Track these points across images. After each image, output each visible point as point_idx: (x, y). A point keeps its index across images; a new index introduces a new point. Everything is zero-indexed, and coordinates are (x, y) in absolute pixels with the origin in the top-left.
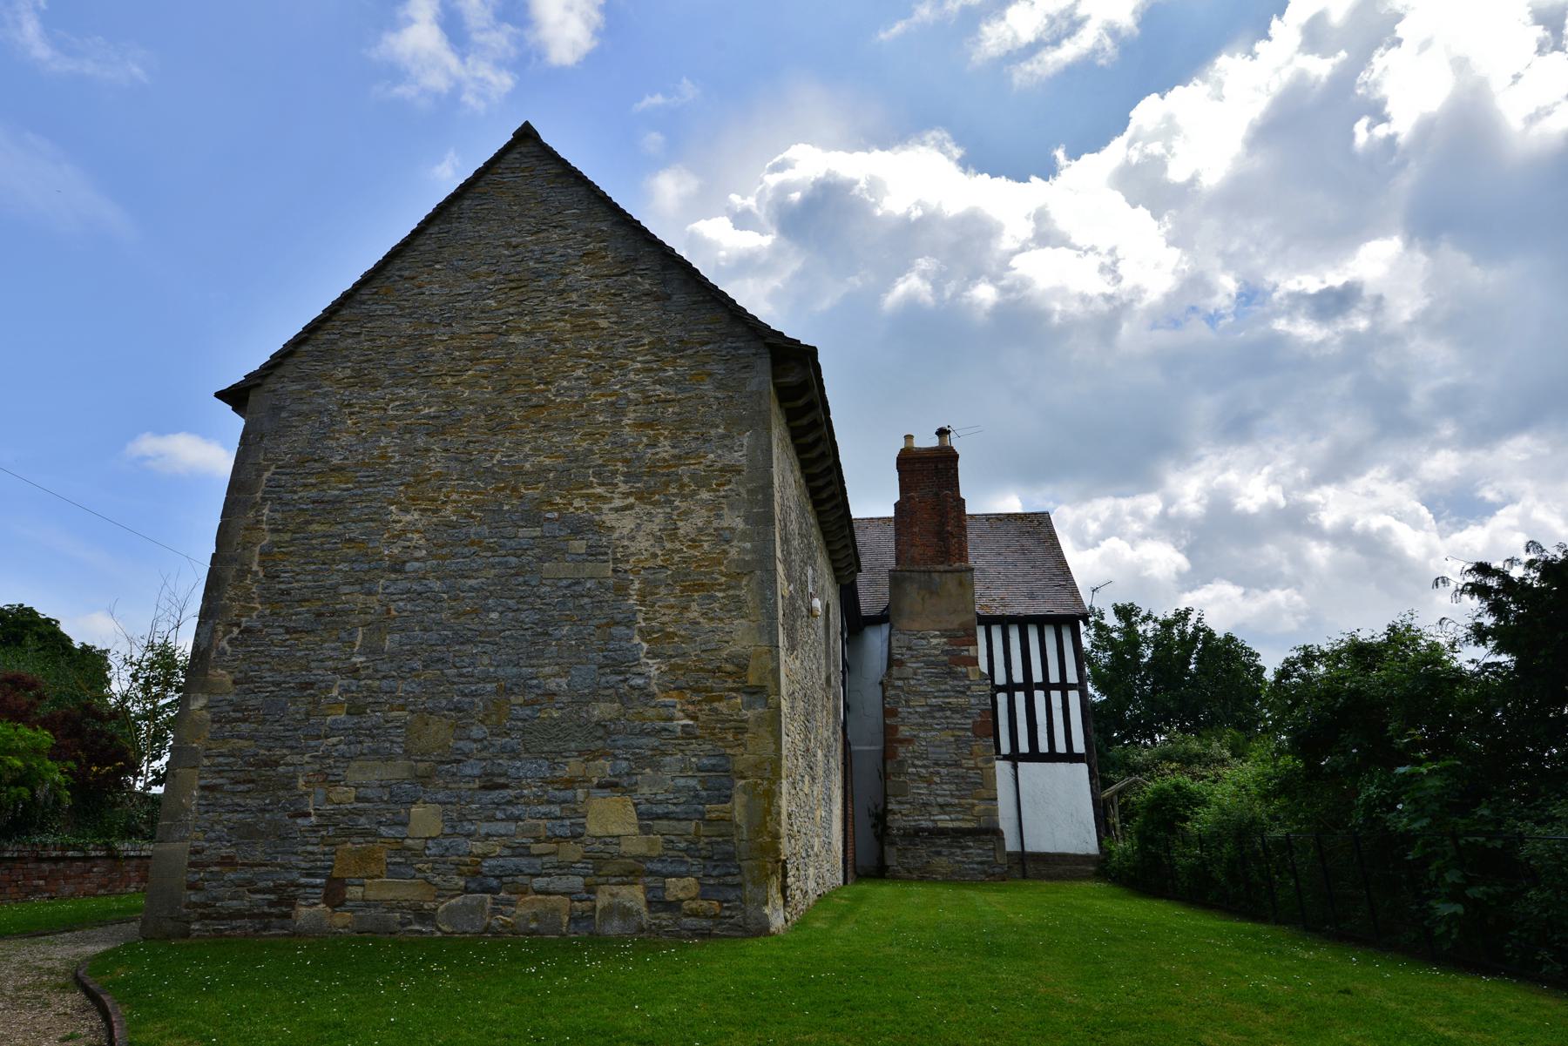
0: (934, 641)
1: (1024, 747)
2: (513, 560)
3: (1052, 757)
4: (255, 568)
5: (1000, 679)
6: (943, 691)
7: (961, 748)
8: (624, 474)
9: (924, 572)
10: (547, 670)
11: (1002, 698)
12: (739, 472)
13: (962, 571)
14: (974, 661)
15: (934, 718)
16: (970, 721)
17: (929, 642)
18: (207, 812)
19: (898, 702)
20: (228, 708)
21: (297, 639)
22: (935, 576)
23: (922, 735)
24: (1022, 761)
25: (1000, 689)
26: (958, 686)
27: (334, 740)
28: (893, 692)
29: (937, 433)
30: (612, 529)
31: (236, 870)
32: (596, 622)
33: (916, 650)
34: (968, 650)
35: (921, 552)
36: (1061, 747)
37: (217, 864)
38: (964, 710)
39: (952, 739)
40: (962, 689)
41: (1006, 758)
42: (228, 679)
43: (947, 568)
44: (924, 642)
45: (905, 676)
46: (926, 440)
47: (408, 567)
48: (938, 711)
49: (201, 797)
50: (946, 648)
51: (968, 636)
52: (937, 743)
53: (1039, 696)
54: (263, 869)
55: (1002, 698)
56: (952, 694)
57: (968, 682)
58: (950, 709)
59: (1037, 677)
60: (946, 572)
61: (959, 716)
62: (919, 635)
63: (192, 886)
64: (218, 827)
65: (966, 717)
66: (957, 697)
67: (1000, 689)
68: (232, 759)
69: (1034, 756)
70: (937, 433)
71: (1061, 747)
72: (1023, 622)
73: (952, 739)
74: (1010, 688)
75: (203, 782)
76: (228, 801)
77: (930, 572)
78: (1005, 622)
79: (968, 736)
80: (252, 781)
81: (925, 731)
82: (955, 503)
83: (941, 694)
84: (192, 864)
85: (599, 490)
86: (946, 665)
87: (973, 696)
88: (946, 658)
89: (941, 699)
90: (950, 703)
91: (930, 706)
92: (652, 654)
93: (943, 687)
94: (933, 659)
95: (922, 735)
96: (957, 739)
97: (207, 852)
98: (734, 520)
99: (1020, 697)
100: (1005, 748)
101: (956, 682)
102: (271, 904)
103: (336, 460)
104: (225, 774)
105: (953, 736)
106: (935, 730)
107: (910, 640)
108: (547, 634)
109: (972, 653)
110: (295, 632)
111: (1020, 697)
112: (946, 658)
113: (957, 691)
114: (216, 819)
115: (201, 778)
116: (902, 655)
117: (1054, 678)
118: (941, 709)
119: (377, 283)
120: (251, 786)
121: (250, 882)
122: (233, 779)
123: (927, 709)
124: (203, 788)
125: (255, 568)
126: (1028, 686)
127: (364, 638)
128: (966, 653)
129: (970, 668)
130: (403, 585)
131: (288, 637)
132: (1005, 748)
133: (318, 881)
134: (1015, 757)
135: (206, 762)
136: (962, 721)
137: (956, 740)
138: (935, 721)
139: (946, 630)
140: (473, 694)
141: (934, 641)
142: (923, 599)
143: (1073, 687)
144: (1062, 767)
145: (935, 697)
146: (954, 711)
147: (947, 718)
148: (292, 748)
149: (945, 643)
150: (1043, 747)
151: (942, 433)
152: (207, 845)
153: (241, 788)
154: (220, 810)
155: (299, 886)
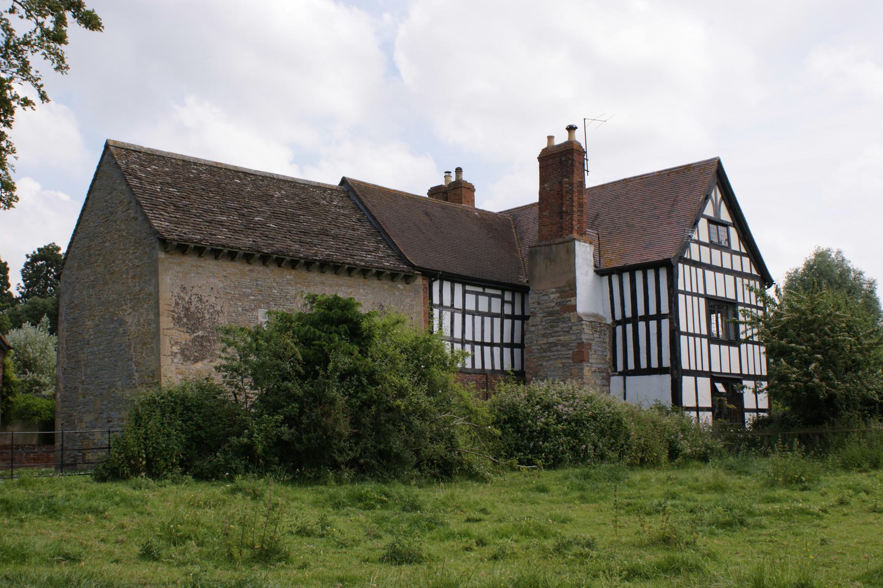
0: (552, 296)
1: (631, 366)
2: (109, 337)
3: (649, 371)
5: (618, 317)
6: (557, 332)
7: (565, 372)
8: (130, 300)
9: (547, 245)
10: (117, 379)
11: (619, 329)
12: (152, 295)
13: (568, 242)
14: (574, 308)
15: (551, 351)
16: (571, 352)
17: (549, 297)
19: (532, 342)
22: (554, 247)
23: (545, 364)
24: (630, 375)
25: (618, 323)
26: (565, 327)
27: (80, 407)
28: (529, 335)
29: (567, 129)
30: (127, 322)
32: (125, 360)
33: (542, 304)
34: (570, 301)
35: (550, 230)
36: (655, 364)
38: (568, 345)
39: (561, 365)
40: (567, 329)
41: (620, 374)
43: (561, 240)
44: (546, 298)
45: (535, 324)
46: (561, 138)
47: (91, 341)
48: (554, 346)
50: (559, 300)
51: (571, 290)
52: (552, 369)
53: (642, 325)
55: (619, 329)
56: (561, 333)
57: (570, 324)
58: (561, 344)
59: (641, 312)
60: (560, 243)
61: (565, 349)
62: (544, 293)
65: (570, 350)
66: (565, 336)
67: (618, 323)
69: (638, 371)
70: (567, 129)
71: (655, 364)
72: (632, 270)
73: (561, 365)
74: (624, 321)
77: (550, 245)
78: (620, 271)
79: (570, 363)
81: (547, 361)
82: (570, 188)
83: (556, 334)
85: (124, 307)
86: (558, 313)
87: (573, 334)
88: (558, 308)
89: (556, 338)
90: (560, 340)
91: (549, 343)
92: (137, 371)
93: (556, 329)
94: (551, 309)
95: (545, 364)
96: (564, 365)
98: (152, 317)
99: (629, 327)
100: (620, 368)
101: (564, 325)
103: (76, 302)
105: (561, 363)
106: (552, 359)
107: (539, 298)
108: (116, 365)
109: (573, 303)
111: (629, 327)
112: (558, 308)
113: (564, 331)
116: (535, 308)
117: (653, 311)
118: (555, 344)
119: (81, 223)
123: (548, 345)
125: (64, 346)
126: (635, 320)
128: (569, 303)
129: (571, 313)
130: (90, 349)
132: (620, 368)
133: (80, 454)
134: (626, 373)
136: (567, 353)
137: (563, 366)
138: (552, 354)
139: (559, 288)
140: (104, 389)
141: (552, 296)
142: (546, 266)
143: (665, 316)
144: (654, 378)
145: (552, 337)
146: (563, 345)
147: (558, 351)
149: (559, 297)
150: (644, 365)
151: (571, 129)
155: (77, 456)
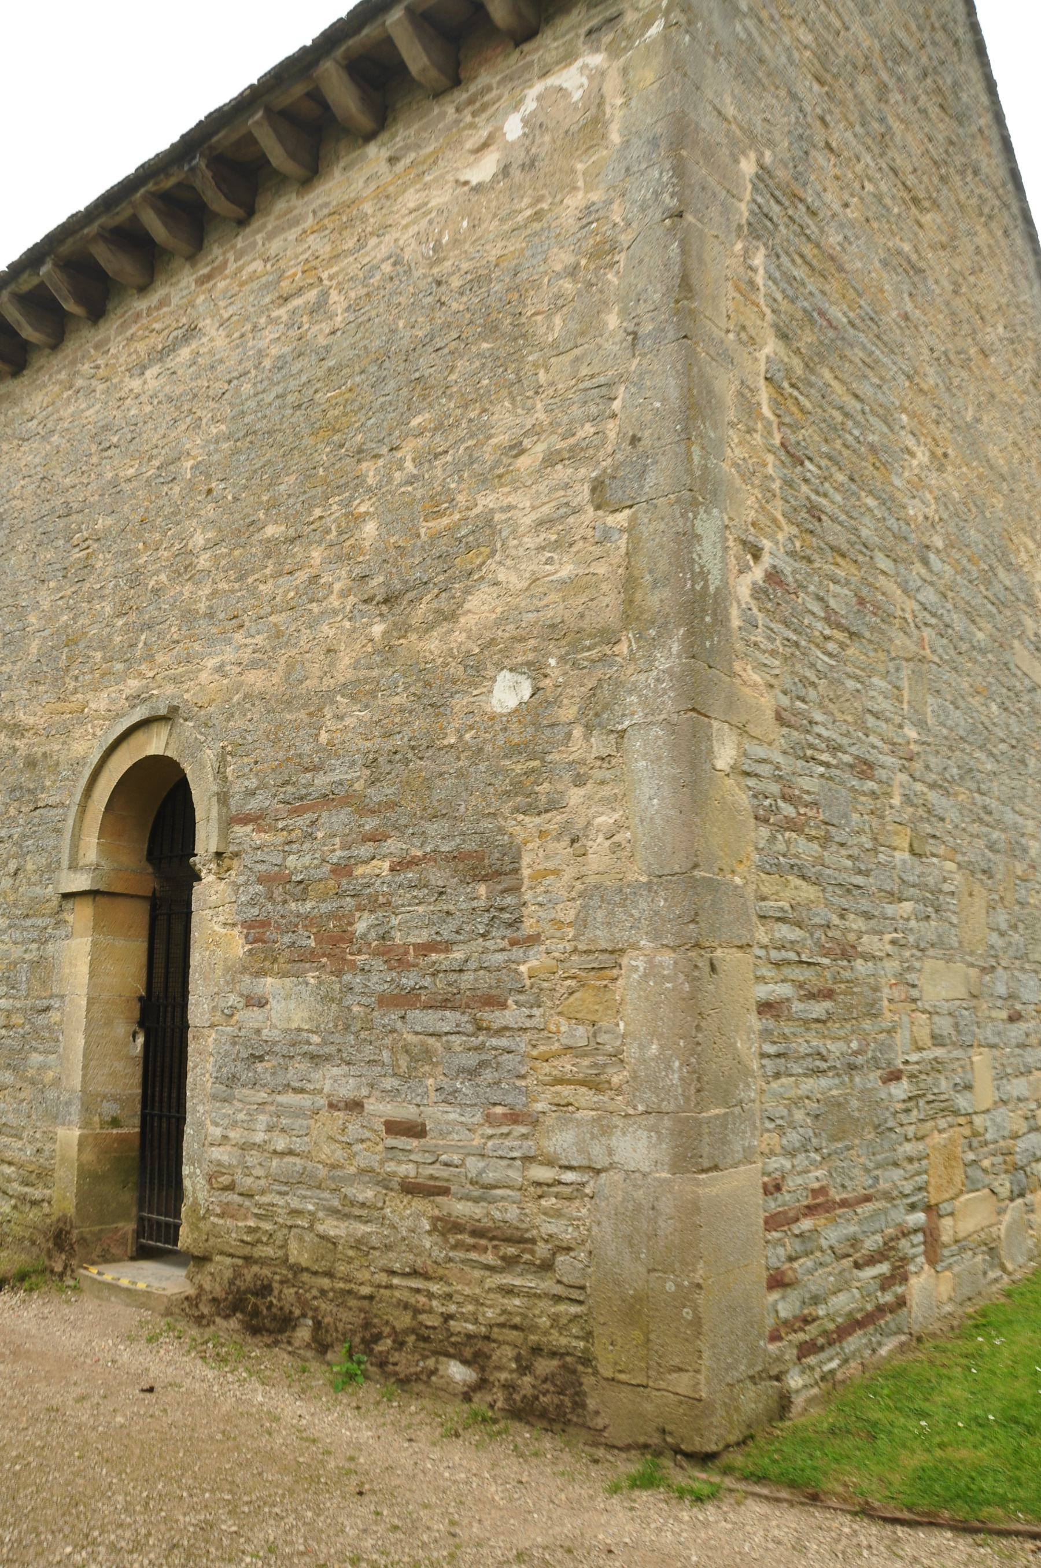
4: (766, 411)
18: (777, 1075)
20: (774, 788)
21: (843, 646)
31: (833, 1221)
37: (811, 1210)
42: (767, 702)
49: (766, 1034)
54: (869, 1207)
63: (778, 1282)
64: (799, 1115)
68: (796, 934)
75: (762, 992)
76: (804, 1049)
80: (829, 994)
84: (773, 1222)
97: (791, 1183)
102: (885, 1283)
104: (787, 971)
110: (839, 626)
114: (793, 1093)
115: (760, 979)
120: (828, 1004)
121: (854, 1242)
122: (801, 986)
124: (766, 1007)
127: (910, 688)
131: (827, 632)
135: (762, 935)
148: (867, 916)
152: (788, 1165)
153: (818, 1009)
154: (797, 1069)
